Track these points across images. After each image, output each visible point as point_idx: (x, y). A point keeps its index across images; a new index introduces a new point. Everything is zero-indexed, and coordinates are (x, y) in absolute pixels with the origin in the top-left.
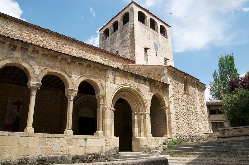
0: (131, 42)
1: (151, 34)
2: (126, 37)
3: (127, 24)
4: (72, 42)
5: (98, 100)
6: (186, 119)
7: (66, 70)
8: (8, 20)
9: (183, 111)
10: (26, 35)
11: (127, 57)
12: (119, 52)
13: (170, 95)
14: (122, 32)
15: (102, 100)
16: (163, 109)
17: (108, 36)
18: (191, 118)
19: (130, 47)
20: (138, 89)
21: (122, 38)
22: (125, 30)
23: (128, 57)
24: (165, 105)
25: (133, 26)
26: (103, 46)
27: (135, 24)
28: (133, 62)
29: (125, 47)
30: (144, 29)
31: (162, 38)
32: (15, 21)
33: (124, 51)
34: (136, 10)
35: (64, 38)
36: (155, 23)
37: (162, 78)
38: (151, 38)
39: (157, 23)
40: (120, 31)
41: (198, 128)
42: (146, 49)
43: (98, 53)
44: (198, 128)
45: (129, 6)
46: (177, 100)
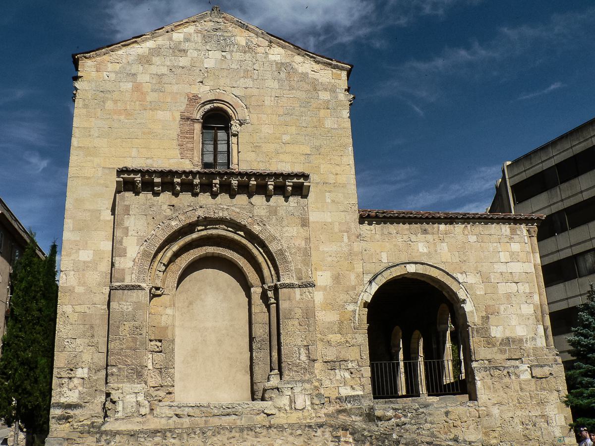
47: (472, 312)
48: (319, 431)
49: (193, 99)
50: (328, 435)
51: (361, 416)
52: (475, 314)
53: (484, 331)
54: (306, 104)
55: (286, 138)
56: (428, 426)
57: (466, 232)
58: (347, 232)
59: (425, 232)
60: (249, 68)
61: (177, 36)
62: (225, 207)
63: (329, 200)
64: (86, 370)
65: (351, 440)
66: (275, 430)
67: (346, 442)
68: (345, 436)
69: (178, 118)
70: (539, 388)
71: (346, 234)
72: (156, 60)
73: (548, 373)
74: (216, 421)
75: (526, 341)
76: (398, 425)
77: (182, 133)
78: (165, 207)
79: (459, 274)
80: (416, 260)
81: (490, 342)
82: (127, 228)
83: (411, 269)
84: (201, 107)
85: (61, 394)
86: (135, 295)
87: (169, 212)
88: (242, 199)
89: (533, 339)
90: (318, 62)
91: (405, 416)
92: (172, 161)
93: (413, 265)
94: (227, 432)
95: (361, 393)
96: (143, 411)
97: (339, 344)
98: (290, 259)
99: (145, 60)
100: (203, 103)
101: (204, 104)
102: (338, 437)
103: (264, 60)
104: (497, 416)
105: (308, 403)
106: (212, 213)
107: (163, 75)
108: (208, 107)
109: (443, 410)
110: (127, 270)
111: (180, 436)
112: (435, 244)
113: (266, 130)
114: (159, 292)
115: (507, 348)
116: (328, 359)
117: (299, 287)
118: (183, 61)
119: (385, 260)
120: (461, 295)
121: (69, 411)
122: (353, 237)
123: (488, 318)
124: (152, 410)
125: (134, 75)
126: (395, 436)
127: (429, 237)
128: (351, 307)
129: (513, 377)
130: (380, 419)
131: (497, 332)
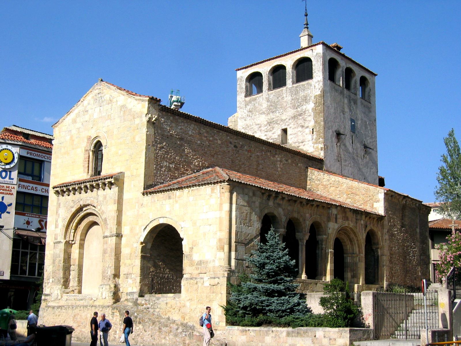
0: (316, 122)
2: (304, 107)
4: (251, 140)
5: (320, 242)
6: (401, 262)
8: (188, 121)
9: (398, 251)
10: (205, 139)
12: (289, 132)
14: (296, 94)
16: (374, 248)
17: (260, 90)
18: (408, 261)
19: (313, 129)
21: (295, 107)
22: (302, 94)
26: (248, 107)
29: (303, 127)
31: (362, 104)
32: (195, 121)
33: (299, 134)
35: (242, 136)
36: (352, 74)
37: (375, 205)
39: (354, 75)
41: (415, 276)
42: (338, 134)
44: (415, 276)
48: (108, 309)
50: (110, 311)
51: (132, 303)
55: (120, 152)
58: (138, 203)
59: (170, 198)
61: (85, 103)
62: (89, 198)
65: (118, 314)
66: (94, 308)
67: (117, 315)
68: (116, 313)
69: (84, 150)
70: (211, 292)
71: (137, 204)
74: (78, 303)
75: (210, 262)
76: (145, 309)
77: (85, 159)
82: (59, 214)
83: (162, 221)
84: (93, 142)
86: (60, 245)
87: (72, 204)
89: (214, 261)
90: (136, 100)
91: (149, 304)
94: (79, 308)
98: (108, 223)
99: (74, 121)
100: (93, 140)
102: (114, 313)
104: (189, 307)
105: (107, 295)
106: (85, 202)
107: (80, 127)
108: (95, 142)
109: (165, 302)
110: (59, 235)
111: (66, 309)
115: (200, 267)
116: (125, 273)
117: (110, 237)
118: (87, 118)
120: (181, 236)
121: (46, 297)
123: (193, 248)
125: (71, 131)
127: (171, 200)
128: (135, 245)
131: (196, 257)
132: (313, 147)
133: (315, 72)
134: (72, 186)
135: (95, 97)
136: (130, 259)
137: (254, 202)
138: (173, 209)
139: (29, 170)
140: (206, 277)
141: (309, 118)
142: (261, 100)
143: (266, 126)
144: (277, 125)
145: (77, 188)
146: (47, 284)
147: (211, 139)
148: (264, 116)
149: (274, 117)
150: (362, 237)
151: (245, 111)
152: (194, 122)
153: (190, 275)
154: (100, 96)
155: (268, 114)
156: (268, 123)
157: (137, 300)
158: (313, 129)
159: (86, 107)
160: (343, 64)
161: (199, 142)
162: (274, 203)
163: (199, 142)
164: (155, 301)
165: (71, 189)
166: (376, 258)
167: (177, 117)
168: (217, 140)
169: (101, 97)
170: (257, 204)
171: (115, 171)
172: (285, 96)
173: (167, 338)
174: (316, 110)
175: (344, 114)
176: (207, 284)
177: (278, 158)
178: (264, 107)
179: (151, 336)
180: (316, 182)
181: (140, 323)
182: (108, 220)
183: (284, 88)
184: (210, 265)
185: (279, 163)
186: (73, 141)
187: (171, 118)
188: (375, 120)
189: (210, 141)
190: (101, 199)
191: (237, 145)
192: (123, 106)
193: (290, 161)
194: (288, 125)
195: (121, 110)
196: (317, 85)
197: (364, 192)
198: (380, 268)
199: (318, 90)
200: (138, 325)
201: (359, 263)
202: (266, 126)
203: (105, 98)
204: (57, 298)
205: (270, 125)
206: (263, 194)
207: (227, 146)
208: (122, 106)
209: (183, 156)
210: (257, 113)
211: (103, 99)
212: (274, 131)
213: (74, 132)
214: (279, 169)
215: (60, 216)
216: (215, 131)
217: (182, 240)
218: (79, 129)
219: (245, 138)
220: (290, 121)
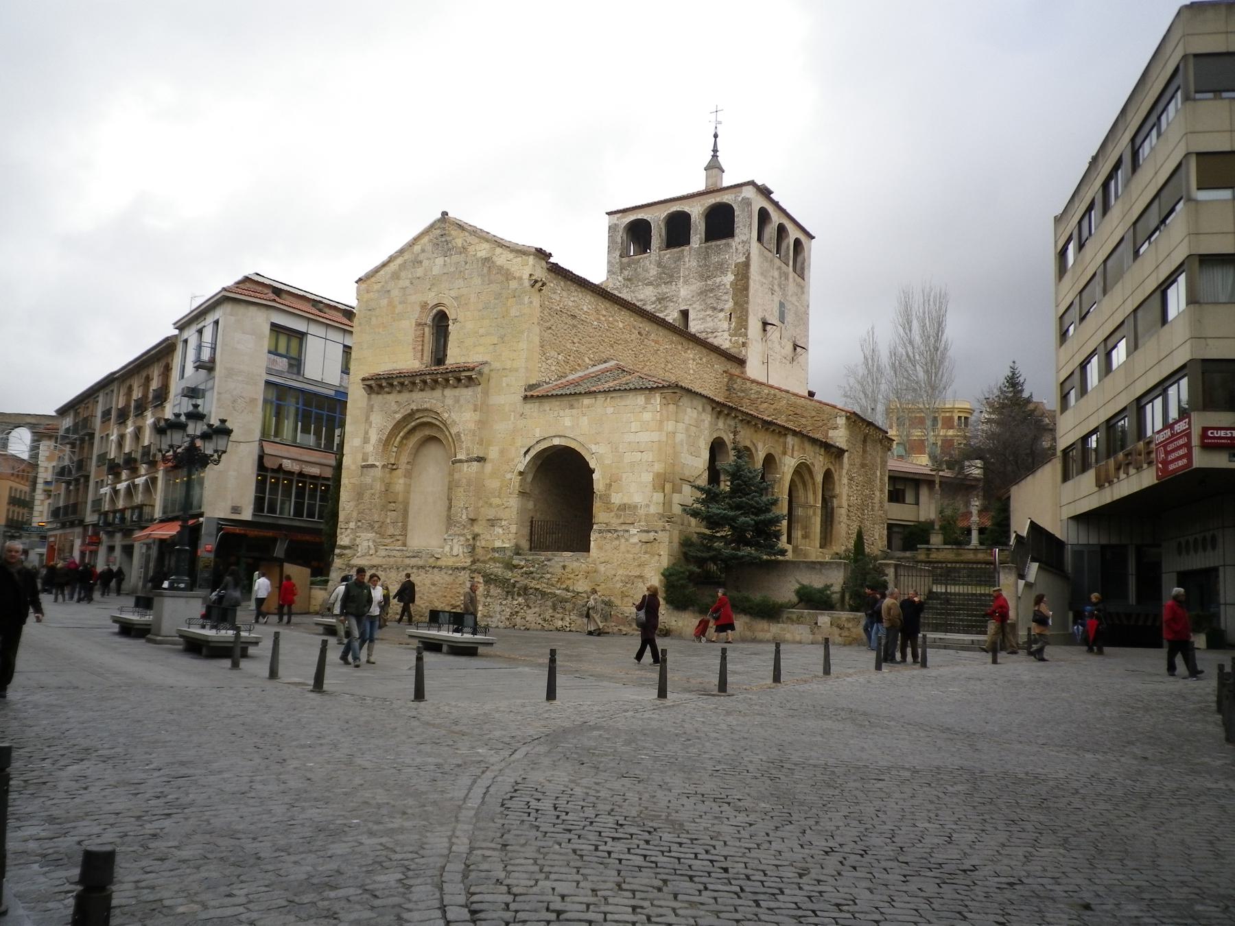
0: (736, 304)
1: (776, 274)
2: (718, 280)
3: (724, 241)
7: (755, 441)
8: (583, 289)
11: (716, 342)
12: (691, 316)
13: (844, 472)
15: (776, 486)
18: (866, 517)
19: (731, 314)
20: (812, 464)
21: (704, 277)
22: (715, 259)
23: (724, 341)
24: (833, 489)
25: (748, 258)
26: (626, 273)
27: (751, 255)
28: (741, 362)
30: (766, 264)
32: (592, 291)
33: (709, 319)
34: (759, 202)
37: (831, 433)
38: (776, 288)
40: (698, 251)
42: (765, 324)
43: (691, 346)
45: (738, 189)
46: (851, 479)
47: (598, 480)
49: (424, 305)
50: (467, 575)
52: (601, 482)
53: (606, 498)
54: (498, 296)
55: (482, 331)
56: (549, 576)
57: (605, 405)
58: (514, 411)
59: (572, 407)
60: (462, 269)
63: (504, 385)
64: (354, 523)
65: (482, 581)
72: (403, 274)
73: (652, 538)
74: (407, 561)
76: (526, 574)
78: (393, 403)
79: (593, 446)
80: (560, 434)
81: (608, 506)
83: (556, 442)
85: (341, 539)
87: (394, 407)
88: (438, 393)
91: (533, 566)
92: (408, 363)
93: (558, 439)
95: (507, 545)
96: (371, 552)
97: (498, 506)
101: (432, 308)
103: (473, 258)
105: (461, 550)
108: (435, 311)
112: (578, 418)
113: (470, 326)
114: (394, 467)
116: (489, 517)
117: (467, 461)
118: (420, 272)
119: (537, 435)
120: (592, 465)
122: (518, 415)
123: (611, 485)
124: (376, 552)
125: (389, 291)
126: (512, 581)
128: (509, 476)
129: (623, 540)
130: (515, 567)
131: (616, 499)
132: (731, 340)
133: (739, 227)
134: (398, 380)
135: (435, 241)
136: (499, 497)
137: (704, 421)
138: (578, 424)
139: (282, 350)
140: (633, 531)
141: (725, 297)
142: (648, 263)
143: (653, 303)
144: (672, 304)
145: (406, 383)
146: (343, 530)
147: (611, 319)
148: (651, 288)
149: (668, 290)
150: (819, 478)
151: (619, 278)
152: (590, 293)
153: (605, 525)
154: (443, 239)
155: (658, 285)
156: (658, 299)
157: (511, 558)
158: (731, 314)
159: (418, 254)
160: (776, 218)
161: (595, 323)
162: (724, 424)
163: (595, 323)
164: (543, 561)
165: (395, 383)
166: (829, 510)
167: (569, 283)
168: (617, 321)
169: (446, 241)
170: (707, 424)
171: (473, 358)
172: (687, 259)
173: (568, 619)
174: (737, 285)
175: (773, 294)
176: (635, 540)
177: (690, 354)
178: (651, 275)
179: (540, 615)
180: (739, 393)
181: (519, 595)
182: (462, 435)
183: (687, 248)
184: (642, 512)
185: (691, 362)
186: (394, 307)
187: (562, 283)
188: (808, 306)
189: (609, 322)
190: (449, 401)
191: (643, 332)
192: (487, 260)
193: (704, 360)
194: (690, 305)
195: (483, 264)
196: (740, 247)
197: (814, 414)
198: (834, 526)
199: (741, 255)
200: (516, 598)
201: (814, 517)
202: (653, 303)
203: (455, 245)
204: (368, 552)
205: (660, 303)
206: (713, 409)
207: (631, 333)
208: (486, 258)
209: (574, 343)
210: (640, 284)
211: (450, 245)
212: (667, 312)
213: (395, 293)
214: (691, 371)
215: (374, 425)
216: (616, 307)
217: (592, 471)
218: (404, 289)
219: (653, 322)
220: (694, 299)
